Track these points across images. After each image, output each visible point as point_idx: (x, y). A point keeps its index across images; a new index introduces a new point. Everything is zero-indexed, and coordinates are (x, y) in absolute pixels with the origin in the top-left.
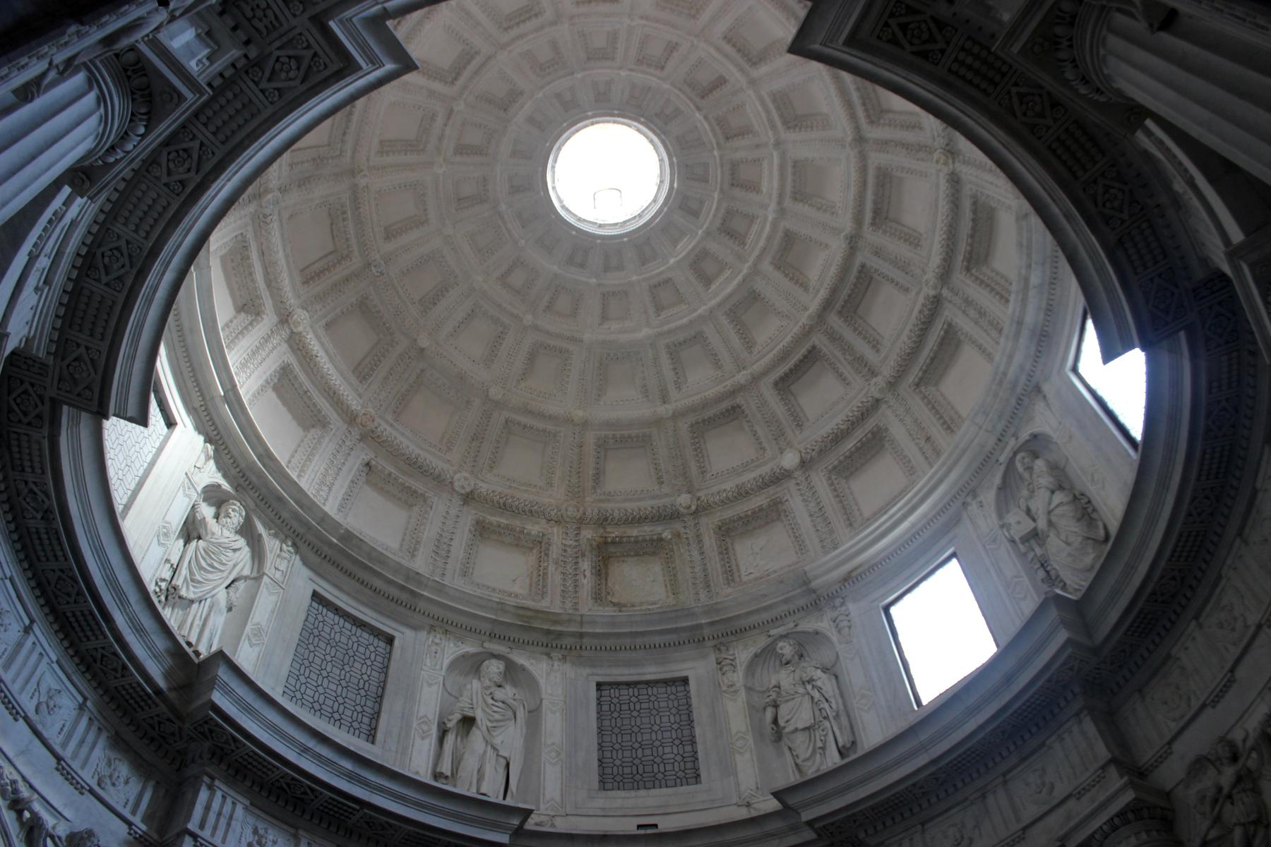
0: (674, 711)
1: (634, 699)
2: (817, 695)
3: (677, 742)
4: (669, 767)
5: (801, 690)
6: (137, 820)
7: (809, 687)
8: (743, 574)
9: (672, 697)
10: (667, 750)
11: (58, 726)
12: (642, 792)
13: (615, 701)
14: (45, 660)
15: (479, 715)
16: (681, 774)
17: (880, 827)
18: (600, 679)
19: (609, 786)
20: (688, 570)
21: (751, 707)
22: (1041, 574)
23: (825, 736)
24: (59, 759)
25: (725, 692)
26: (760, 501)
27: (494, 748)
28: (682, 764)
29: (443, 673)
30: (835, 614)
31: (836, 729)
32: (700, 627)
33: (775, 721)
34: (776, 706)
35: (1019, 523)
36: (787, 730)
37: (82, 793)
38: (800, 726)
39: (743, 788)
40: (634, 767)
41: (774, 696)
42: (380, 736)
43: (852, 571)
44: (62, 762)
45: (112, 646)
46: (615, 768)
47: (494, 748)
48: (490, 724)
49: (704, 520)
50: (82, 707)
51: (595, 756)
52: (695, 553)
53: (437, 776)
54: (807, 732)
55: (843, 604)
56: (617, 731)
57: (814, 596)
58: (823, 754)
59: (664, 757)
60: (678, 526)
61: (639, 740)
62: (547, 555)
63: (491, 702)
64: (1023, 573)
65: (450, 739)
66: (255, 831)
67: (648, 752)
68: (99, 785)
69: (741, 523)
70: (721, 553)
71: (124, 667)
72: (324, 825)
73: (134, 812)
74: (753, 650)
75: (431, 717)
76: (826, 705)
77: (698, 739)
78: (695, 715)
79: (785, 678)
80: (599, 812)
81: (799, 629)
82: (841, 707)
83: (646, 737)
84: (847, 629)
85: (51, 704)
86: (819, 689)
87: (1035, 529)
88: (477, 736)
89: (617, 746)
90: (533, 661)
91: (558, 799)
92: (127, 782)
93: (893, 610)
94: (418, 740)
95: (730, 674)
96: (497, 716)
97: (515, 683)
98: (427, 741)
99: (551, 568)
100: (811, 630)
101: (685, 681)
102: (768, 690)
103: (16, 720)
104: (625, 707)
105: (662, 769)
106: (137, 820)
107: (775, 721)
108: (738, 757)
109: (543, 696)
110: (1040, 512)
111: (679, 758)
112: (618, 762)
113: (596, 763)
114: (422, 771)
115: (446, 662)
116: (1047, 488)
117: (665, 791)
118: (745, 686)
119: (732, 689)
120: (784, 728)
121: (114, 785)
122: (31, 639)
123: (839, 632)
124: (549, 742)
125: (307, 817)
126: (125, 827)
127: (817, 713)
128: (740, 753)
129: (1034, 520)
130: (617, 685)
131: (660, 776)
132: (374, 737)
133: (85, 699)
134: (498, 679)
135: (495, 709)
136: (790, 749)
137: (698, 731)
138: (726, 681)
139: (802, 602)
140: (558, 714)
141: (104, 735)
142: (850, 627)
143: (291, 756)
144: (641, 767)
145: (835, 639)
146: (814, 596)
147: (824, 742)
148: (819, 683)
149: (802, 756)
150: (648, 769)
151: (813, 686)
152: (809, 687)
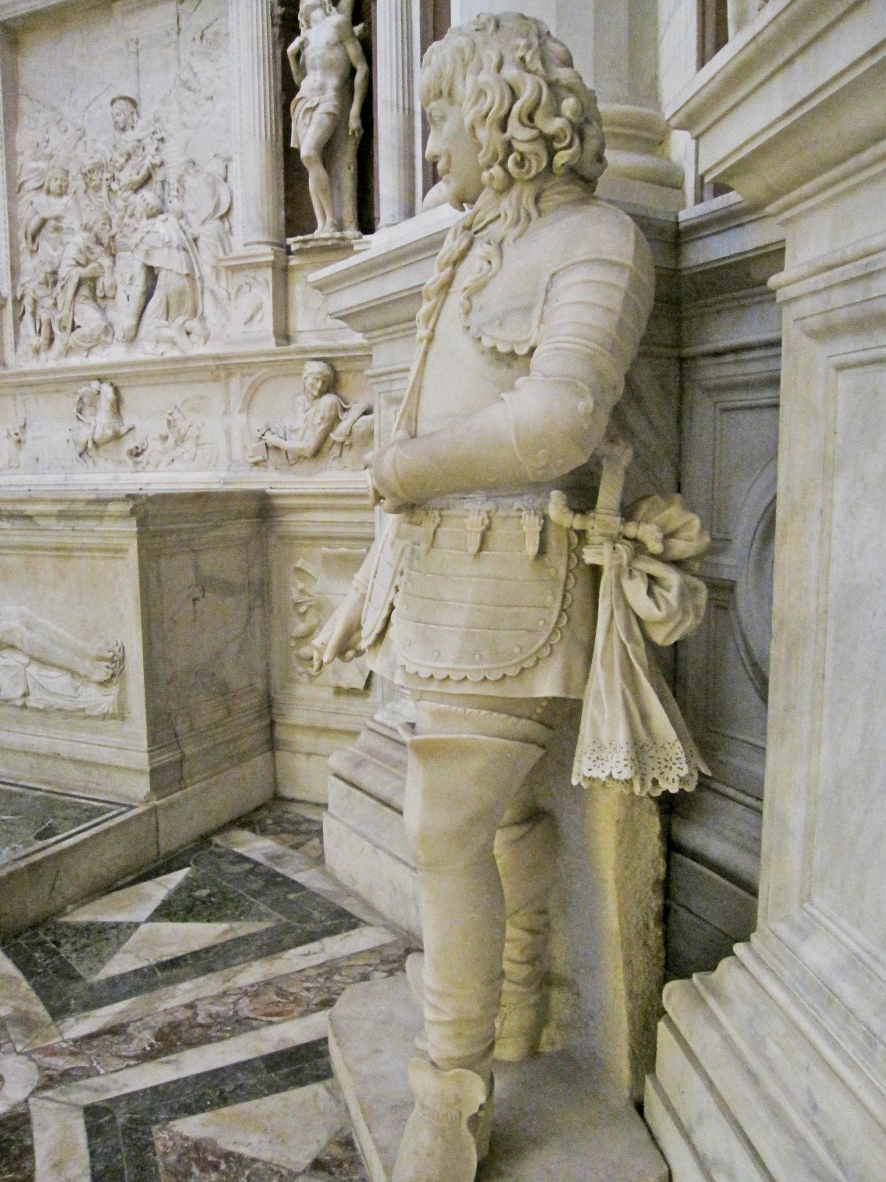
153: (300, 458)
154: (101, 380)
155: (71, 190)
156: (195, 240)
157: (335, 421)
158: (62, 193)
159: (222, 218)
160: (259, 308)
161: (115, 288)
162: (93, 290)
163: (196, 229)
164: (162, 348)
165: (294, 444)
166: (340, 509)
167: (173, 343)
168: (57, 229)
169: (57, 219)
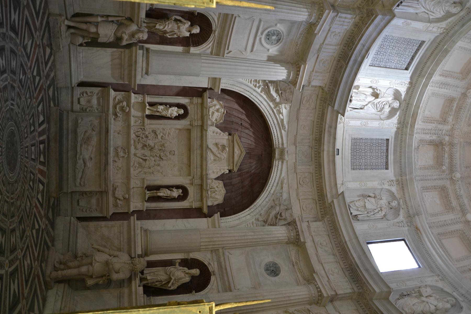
0: (377, 164)
1: (382, 151)
2: (376, 211)
3: (366, 164)
4: (358, 161)
5: (379, 206)
7: (379, 209)
8: (426, 193)
9: (382, 164)
10: (364, 161)
12: (350, 151)
13: (382, 145)
15: (378, 100)
16: (355, 164)
17: (329, 222)
18: (390, 140)
19: (353, 141)
20: (429, 174)
21: (375, 189)
22: (405, 293)
23: (362, 212)
25: (382, 181)
26: (454, 203)
27: (367, 105)
28: (358, 165)
29: (395, 87)
30: (405, 222)
31: (364, 215)
32: (406, 176)
33: (369, 196)
34: (374, 197)
35: (426, 291)
36: (365, 200)
38: (366, 204)
39: (348, 183)
40: (358, 149)
41: (378, 197)
42: (372, 67)
43: (419, 231)
46: (359, 143)
47: (367, 105)
48: (375, 103)
49: (448, 182)
51: (363, 137)
52: (435, 177)
53: (358, 87)
54: (364, 206)
55: (408, 225)
56: (372, 144)
57: (412, 216)
58: (356, 210)
59: (361, 159)
60: (447, 172)
61: (368, 152)
62: (439, 124)
63: (383, 104)
64: (406, 287)
65: (371, 90)
66: (339, 33)
67: (363, 154)
69: (446, 195)
70: (435, 186)
72: (341, 53)
74: (396, 193)
75: (379, 84)
76: (372, 214)
77: (366, 171)
78: (375, 171)
79: (384, 202)
80: (344, 138)
81: (401, 209)
82: (371, 218)
83: (369, 154)
84: (398, 225)
86: (378, 212)
87: (423, 296)
88: (372, 99)
89: (366, 144)
90: (398, 118)
91: (350, 125)
93: (403, 242)
94: (370, 80)
95: (388, 184)
96: (378, 105)
97: (390, 112)
98: (370, 83)
99: (434, 125)
100: (400, 213)
101: (387, 169)
102: (380, 195)
104: (380, 148)
105: (357, 158)
107: (369, 196)
108: (358, 183)
109: (385, 121)
110: (428, 299)
111: (360, 164)
112: (361, 144)
113: (361, 137)
114: (359, 82)
115: (398, 88)
116: (437, 305)
117: (350, 158)
118: (383, 188)
119: (382, 184)
120: (366, 199)
123: (398, 222)
124: (369, 122)
125: (344, 48)
127: (370, 210)
128: (360, 184)
129: (426, 297)
130: (387, 145)
131: (355, 157)
132: (372, 66)
134: (392, 106)
135: (381, 105)
136: (359, 200)
137: (369, 171)
138: (385, 182)
139: (411, 212)
140: (378, 126)
142: (399, 226)
143: (361, 42)
144: (359, 151)
145: (395, 220)
146: (412, 216)
147: (360, 211)
148: (380, 213)
149: (356, 203)
150: (358, 154)
151: (379, 211)
152: (379, 209)
153: (114, 194)
154: (128, 155)
155: (162, 140)
156: (150, 168)
157: (119, 200)
158: (161, 138)
159: (153, 173)
160: (137, 185)
161: (144, 150)
162: (144, 146)
163: (152, 169)
164: (133, 162)
165: (117, 192)
166: (106, 203)
167: (134, 164)
168: (156, 138)
169: (157, 138)
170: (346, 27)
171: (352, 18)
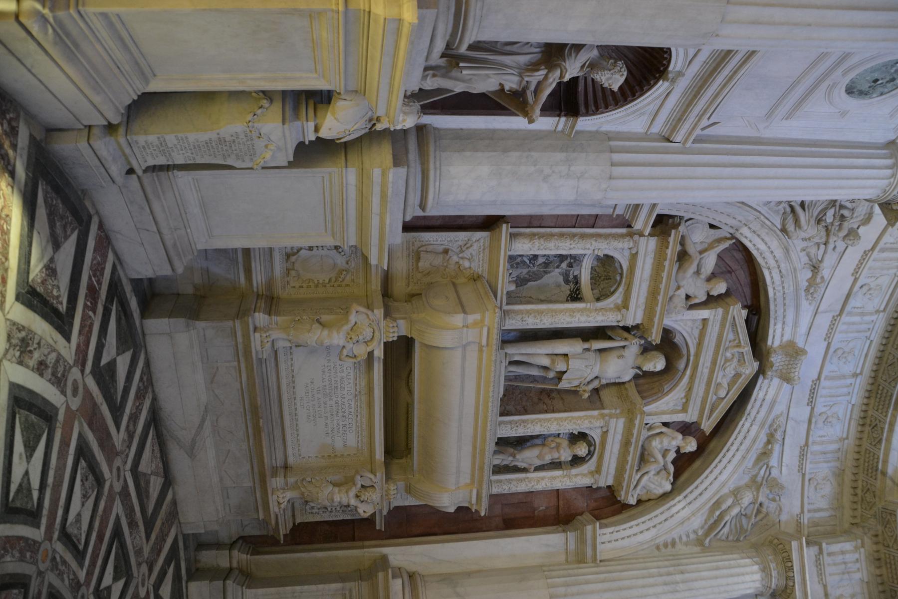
6: (807, 516)
11: (821, 433)
14: (848, 398)
24: (807, 444)
37: (799, 472)
44: (806, 448)
45: (885, 423)
50: (842, 440)
68: (810, 480)
71: (880, 441)
73: (809, 511)
85: (829, 420)
92: (822, 497)
103: (808, 405)
106: (807, 516)
121: (816, 489)
122: (852, 381)
126: (797, 510)
133: (847, 438)
141: (837, 464)
170: (858, 576)
171: (856, 548)
